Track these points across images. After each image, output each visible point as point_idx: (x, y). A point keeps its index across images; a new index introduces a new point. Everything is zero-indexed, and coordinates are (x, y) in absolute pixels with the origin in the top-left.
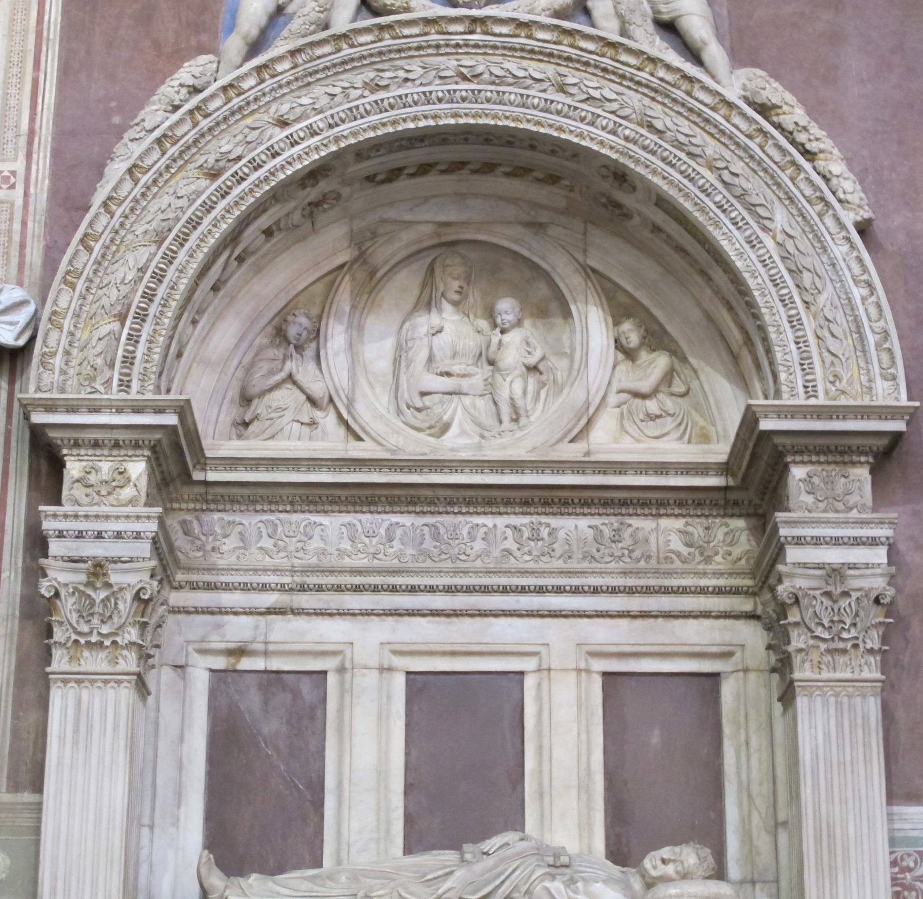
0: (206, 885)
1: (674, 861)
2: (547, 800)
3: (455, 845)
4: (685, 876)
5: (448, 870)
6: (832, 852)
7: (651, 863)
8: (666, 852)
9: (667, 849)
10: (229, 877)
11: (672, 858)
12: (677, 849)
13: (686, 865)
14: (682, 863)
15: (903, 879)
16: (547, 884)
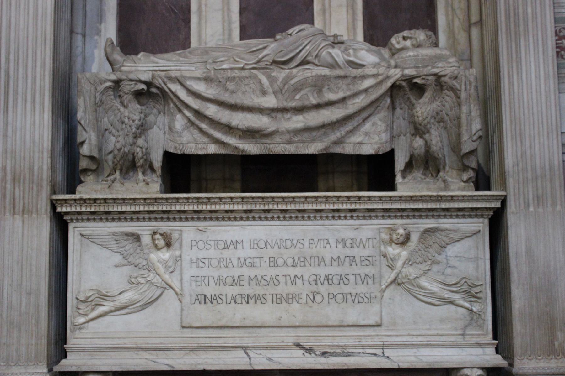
0: (111, 59)
1: (411, 38)
2: (327, 14)
3: (272, 36)
4: (419, 46)
5: (265, 45)
6: (517, 25)
7: (396, 41)
8: (406, 33)
9: (406, 32)
10: (126, 54)
11: (410, 36)
12: (412, 31)
13: (418, 40)
14: (416, 39)
15: (561, 44)
16: (330, 50)
